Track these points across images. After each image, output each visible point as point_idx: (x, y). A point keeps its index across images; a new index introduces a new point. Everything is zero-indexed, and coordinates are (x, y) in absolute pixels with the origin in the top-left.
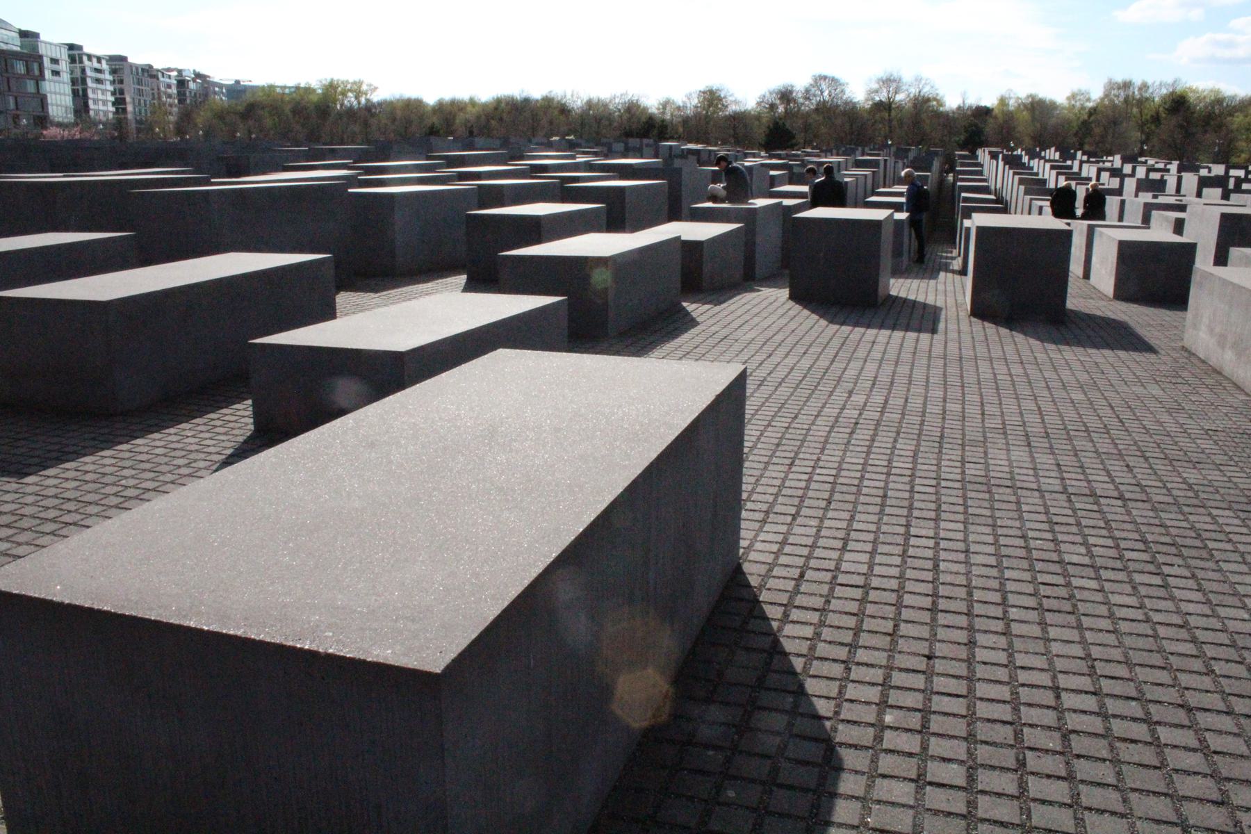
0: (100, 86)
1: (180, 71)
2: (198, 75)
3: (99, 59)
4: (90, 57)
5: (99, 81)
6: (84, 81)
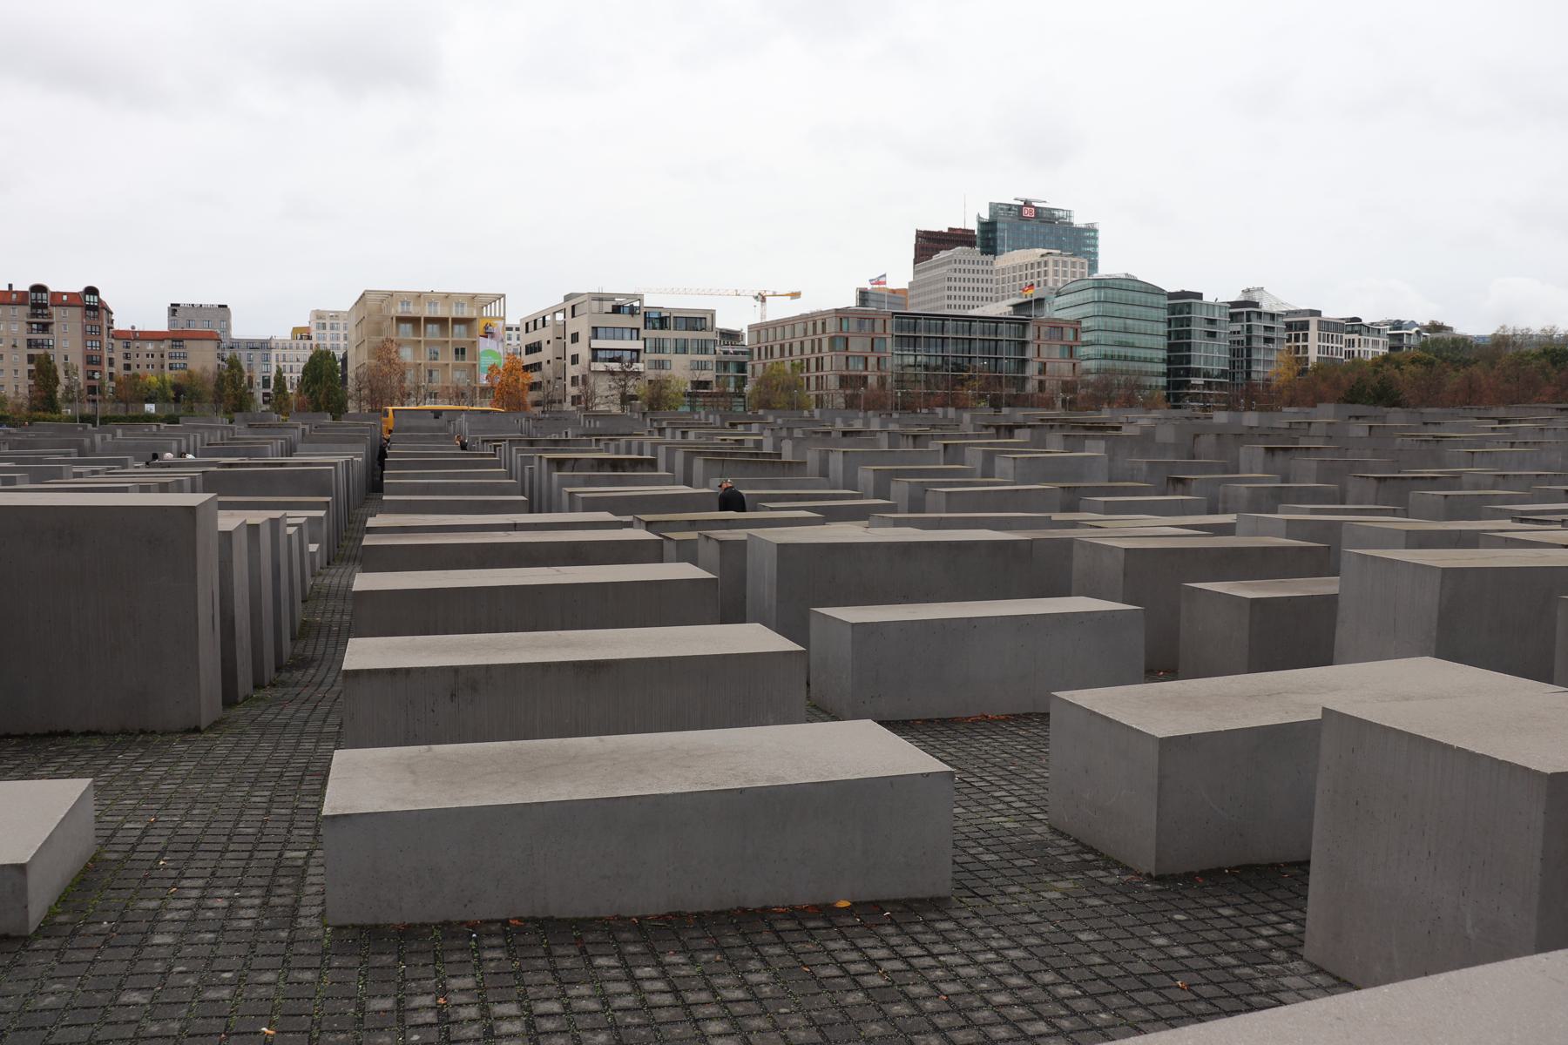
1: (1398, 325)
2: (1436, 327)
3: (1273, 316)
4: (1260, 314)
6: (1249, 339)
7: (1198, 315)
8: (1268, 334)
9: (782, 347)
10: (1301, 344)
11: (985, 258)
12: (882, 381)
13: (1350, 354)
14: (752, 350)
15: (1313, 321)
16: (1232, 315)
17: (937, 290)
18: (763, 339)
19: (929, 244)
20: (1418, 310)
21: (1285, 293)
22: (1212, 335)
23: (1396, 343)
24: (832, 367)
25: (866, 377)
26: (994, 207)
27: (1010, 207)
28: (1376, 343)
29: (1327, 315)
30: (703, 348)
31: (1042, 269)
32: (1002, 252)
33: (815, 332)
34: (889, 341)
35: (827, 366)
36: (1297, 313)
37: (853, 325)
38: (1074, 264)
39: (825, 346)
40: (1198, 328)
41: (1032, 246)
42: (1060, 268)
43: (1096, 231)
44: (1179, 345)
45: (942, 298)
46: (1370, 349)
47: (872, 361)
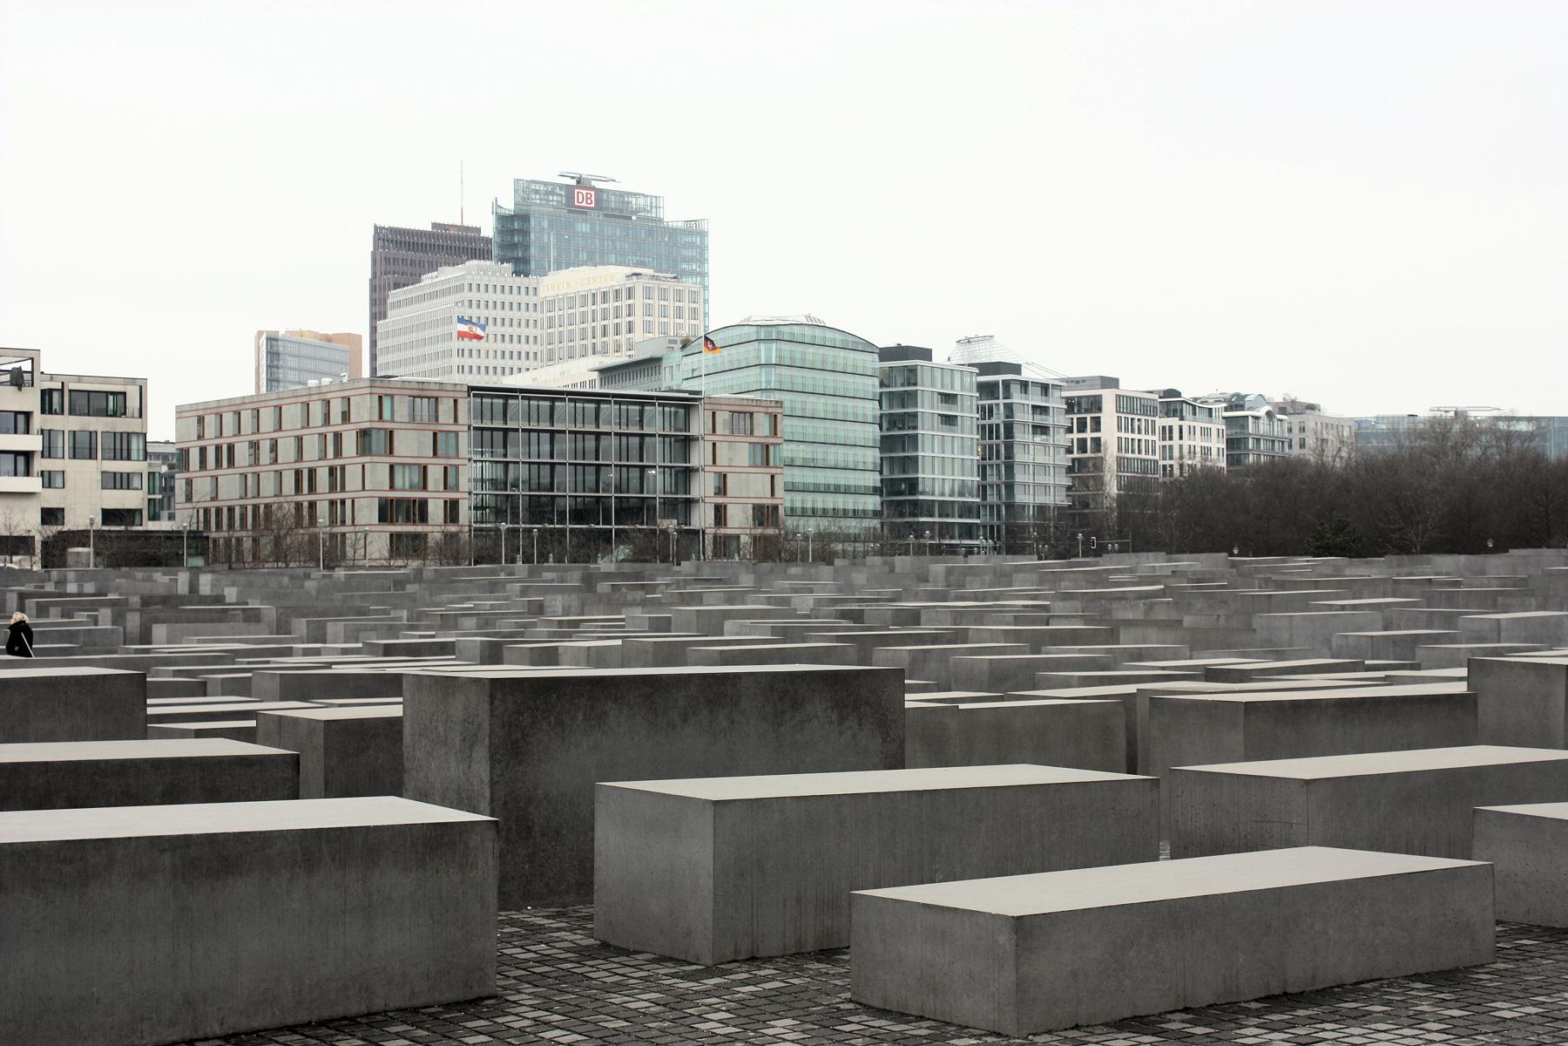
0: (1038, 439)
1: (1237, 402)
3: (1045, 388)
4: (1024, 385)
5: (1042, 429)
6: (1009, 428)
7: (927, 388)
8: (1039, 419)
9: (255, 446)
10: (1088, 435)
11: (522, 281)
12: (452, 509)
13: (1167, 452)
14: (184, 454)
15: (1108, 397)
16: (982, 387)
17: (437, 339)
18: (210, 430)
19: (404, 256)
20: (1266, 383)
21: (1049, 356)
22: (949, 420)
23: (1236, 432)
24: (368, 483)
25: (423, 504)
26: (525, 189)
27: (551, 188)
28: (1206, 432)
29: (1131, 384)
30: (121, 447)
31: (624, 303)
32: (543, 272)
33: (327, 420)
34: (464, 438)
35: (353, 480)
36: (1077, 382)
37: (402, 408)
38: (679, 295)
39: (350, 444)
40: (928, 408)
41: (592, 261)
42: (655, 302)
43: (703, 234)
44: (898, 437)
45: (447, 354)
46: (1199, 443)
47: (435, 474)
